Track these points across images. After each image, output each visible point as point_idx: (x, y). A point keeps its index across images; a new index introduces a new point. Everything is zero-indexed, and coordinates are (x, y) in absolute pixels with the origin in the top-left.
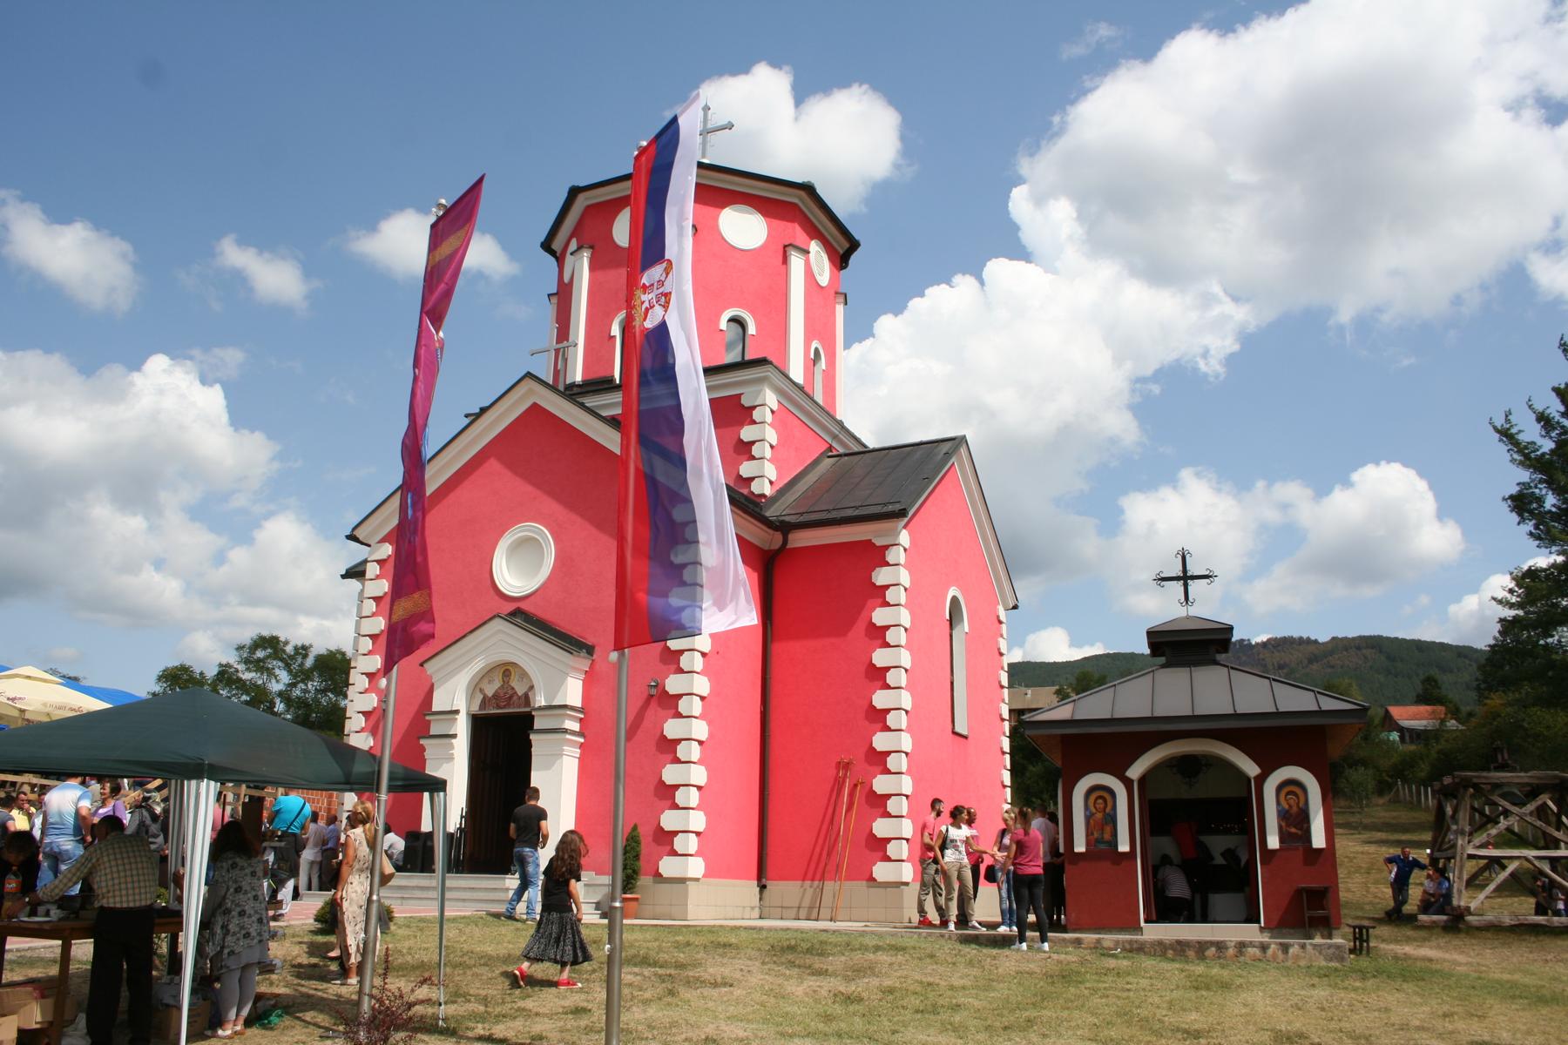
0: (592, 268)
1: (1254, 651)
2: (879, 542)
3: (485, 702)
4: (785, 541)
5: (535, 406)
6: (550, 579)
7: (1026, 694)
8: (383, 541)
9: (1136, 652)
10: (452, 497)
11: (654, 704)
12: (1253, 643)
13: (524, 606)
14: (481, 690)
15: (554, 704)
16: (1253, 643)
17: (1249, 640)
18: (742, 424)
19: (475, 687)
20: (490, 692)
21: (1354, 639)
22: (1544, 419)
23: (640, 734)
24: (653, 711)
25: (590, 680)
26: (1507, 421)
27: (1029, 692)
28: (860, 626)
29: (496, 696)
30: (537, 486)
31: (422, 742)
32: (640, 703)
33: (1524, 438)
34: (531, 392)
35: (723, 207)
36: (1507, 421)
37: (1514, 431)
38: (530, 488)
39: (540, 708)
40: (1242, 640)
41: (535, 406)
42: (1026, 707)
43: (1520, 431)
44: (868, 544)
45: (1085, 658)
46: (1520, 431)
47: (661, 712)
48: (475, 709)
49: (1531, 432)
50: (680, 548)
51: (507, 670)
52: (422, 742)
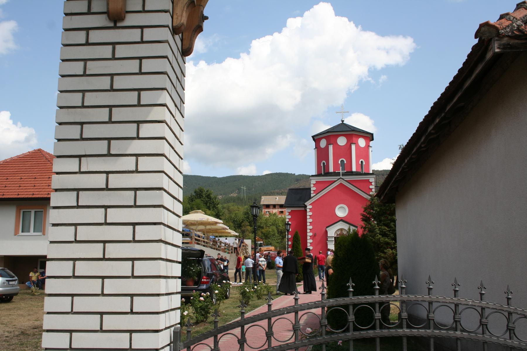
3: (337, 235)
6: (348, 214)
7: (276, 198)
8: (310, 205)
9: (289, 172)
14: (336, 233)
20: (338, 233)
21: (381, 171)
29: (340, 234)
31: (327, 242)
34: (341, 181)
41: (341, 183)
42: (277, 204)
45: (266, 174)
48: (336, 236)
51: (341, 230)
52: (327, 242)
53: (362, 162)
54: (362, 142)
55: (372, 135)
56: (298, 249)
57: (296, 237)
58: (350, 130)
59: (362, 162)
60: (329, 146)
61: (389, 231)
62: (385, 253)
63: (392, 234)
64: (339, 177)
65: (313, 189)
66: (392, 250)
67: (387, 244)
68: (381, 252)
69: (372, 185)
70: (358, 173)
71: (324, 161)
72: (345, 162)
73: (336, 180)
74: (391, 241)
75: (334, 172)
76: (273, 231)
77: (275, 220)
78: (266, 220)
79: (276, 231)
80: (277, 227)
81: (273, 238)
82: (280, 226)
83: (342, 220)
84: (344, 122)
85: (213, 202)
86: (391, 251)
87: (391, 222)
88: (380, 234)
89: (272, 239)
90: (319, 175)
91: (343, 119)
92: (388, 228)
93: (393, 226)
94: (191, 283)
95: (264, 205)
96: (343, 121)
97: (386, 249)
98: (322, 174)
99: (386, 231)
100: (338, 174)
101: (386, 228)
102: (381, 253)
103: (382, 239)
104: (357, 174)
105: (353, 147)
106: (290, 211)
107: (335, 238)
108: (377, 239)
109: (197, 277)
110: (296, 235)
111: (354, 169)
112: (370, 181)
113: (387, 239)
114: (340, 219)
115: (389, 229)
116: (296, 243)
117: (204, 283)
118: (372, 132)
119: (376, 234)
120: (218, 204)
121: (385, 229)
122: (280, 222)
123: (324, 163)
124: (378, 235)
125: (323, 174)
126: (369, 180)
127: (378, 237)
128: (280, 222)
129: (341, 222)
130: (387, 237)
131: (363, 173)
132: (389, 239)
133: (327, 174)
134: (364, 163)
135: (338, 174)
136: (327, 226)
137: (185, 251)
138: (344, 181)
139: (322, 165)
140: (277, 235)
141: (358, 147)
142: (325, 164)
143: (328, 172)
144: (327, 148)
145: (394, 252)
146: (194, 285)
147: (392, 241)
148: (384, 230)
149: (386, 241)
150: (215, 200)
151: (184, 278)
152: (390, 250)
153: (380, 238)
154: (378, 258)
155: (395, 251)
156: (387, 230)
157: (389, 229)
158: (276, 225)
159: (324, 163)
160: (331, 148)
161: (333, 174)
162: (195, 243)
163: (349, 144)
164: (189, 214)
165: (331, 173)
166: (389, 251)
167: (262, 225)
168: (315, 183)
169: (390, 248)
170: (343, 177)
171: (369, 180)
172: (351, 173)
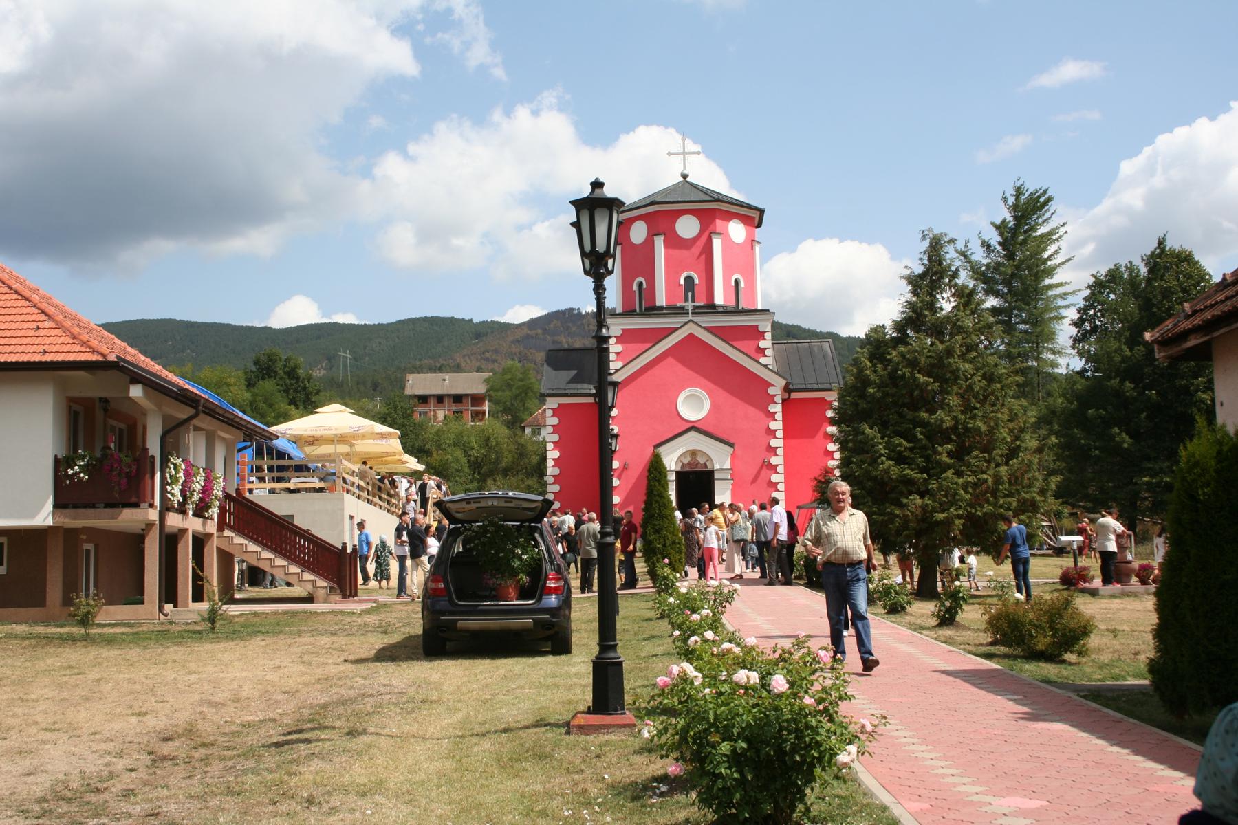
0: (666, 246)
1: (584, 321)
2: (828, 399)
3: (683, 466)
4: (789, 396)
5: (691, 336)
7: (444, 380)
9: (458, 316)
10: (650, 372)
11: (765, 468)
12: (583, 313)
13: (696, 425)
15: (724, 468)
16: (583, 313)
17: (579, 309)
18: (758, 340)
19: (679, 459)
20: (686, 461)
22: (986, 246)
23: (759, 479)
24: (764, 472)
25: (733, 457)
26: (966, 246)
27: (447, 378)
28: (821, 434)
29: (689, 463)
30: (697, 372)
32: (759, 467)
33: (974, 258)
35: (729, 220)
36: (966, 246)
37: (969, 253)
38: (691, 372)
39: (717, 470)
40: (572, 309)
41: (691, 336)
42: (446, 393)
43: (972, 253)
44: (823, 399)
45: (400, 321)
46: (972, 253)
47: (769, 472)
48: (679, 469)
49: (979, 256)
50: (772, 405)
51: (694, 453)
53: (737, 281)
54: (737, 231)
55: (762, 212)
56: (664, 498)
57: (656, 469)
58: (709, 198)
59: (737, 281)
60: (656, 238)
61: (911, 449)
62: (902, 506)
63: (920, 457)
64: (686, 320)
65: (614, 347)
66: (922, 497)
67: (908, 482)
68: (892, 504)
69: (765, 339)
70: (729, 309)
71: (641, 279)
72: (697, 281)
73: (678, 326)
74: (920, 475)
75: (668, 308)
76: (457, 460)
77: (461, 434)
78: (437, 433)
79: (464, 460)
80: (465, 451)
81: (457, 478)
82: (473, 449)
83: (693, 427)
84: (687, 179)
85: (305, 389)
86: (919, 502)
87: (915, 428)
88: (889, 458)
89: (456, 481)
90: (628, 312)
91: (686, 172)
92: (909, 442)
93: (922, 437)
94: (512, 592)
95: (410, 396)
96: (685, 176)
97: (902, 494)
98: (635, 311)
99: (902, 449)
100: (680, 311)
101: (905, 443)
102: (893, 507)
103: (895, 471)
104: (726, 311)
105: (717, 243)
106: (556, 406)
107: (678, 474)
108: (884, 470)
109: (528, 574)
110: (657, 463)
111: (719, 300)
112: (761, 329)
113: (906, 472)
114: (689, 425)
115: (912, 445)
116: (657, 484)
117: (551, 591)
118: (761, 206)
119: (879, 457)
120: (317, 393)
121: (900, 445)
122: (473, 439)
123: (640, 284)
124: (882, 460)
125: (638, 311)
126: (757, 326)
127: (885, 466)
128: (473, 439)
129: (692, 434)
130: (909, 464)
131: (740, 308)
132: (913, 470)
133: (651, 310)
134: (742, 284)
135: (680, 311)
136: (658, 442)
137: (506, 502)
138: (697, 328)
139: (635, 288)
140: (467, 470)
141: (728, 244)
142: (644, 286)
143: (650, 305)
144: (649, 244)
145: (928, 502)
146: (517, 599)
147: (922, 473)
148: (899, 448)
149: (905, 476)
150: (309, 382)
151: (494, 580)
152: (918, 497)
153: (889, 468)
154: (886, 518)
155: (929, 500)
156: (906, 448)
157: (912, 445)
158: (464, 445)
159: (640, 284)
160: (659, 242)
161: (665, 312)
162: (343, 491)
163: (706, 234)
164: (317, 413)
165: (661, 308)
166: (914, 499)
167: (427, 447)
168: (619, 333)
169: (916, 493)
170: (696, 319)
171: (757, 326)
172: (711, 308)
